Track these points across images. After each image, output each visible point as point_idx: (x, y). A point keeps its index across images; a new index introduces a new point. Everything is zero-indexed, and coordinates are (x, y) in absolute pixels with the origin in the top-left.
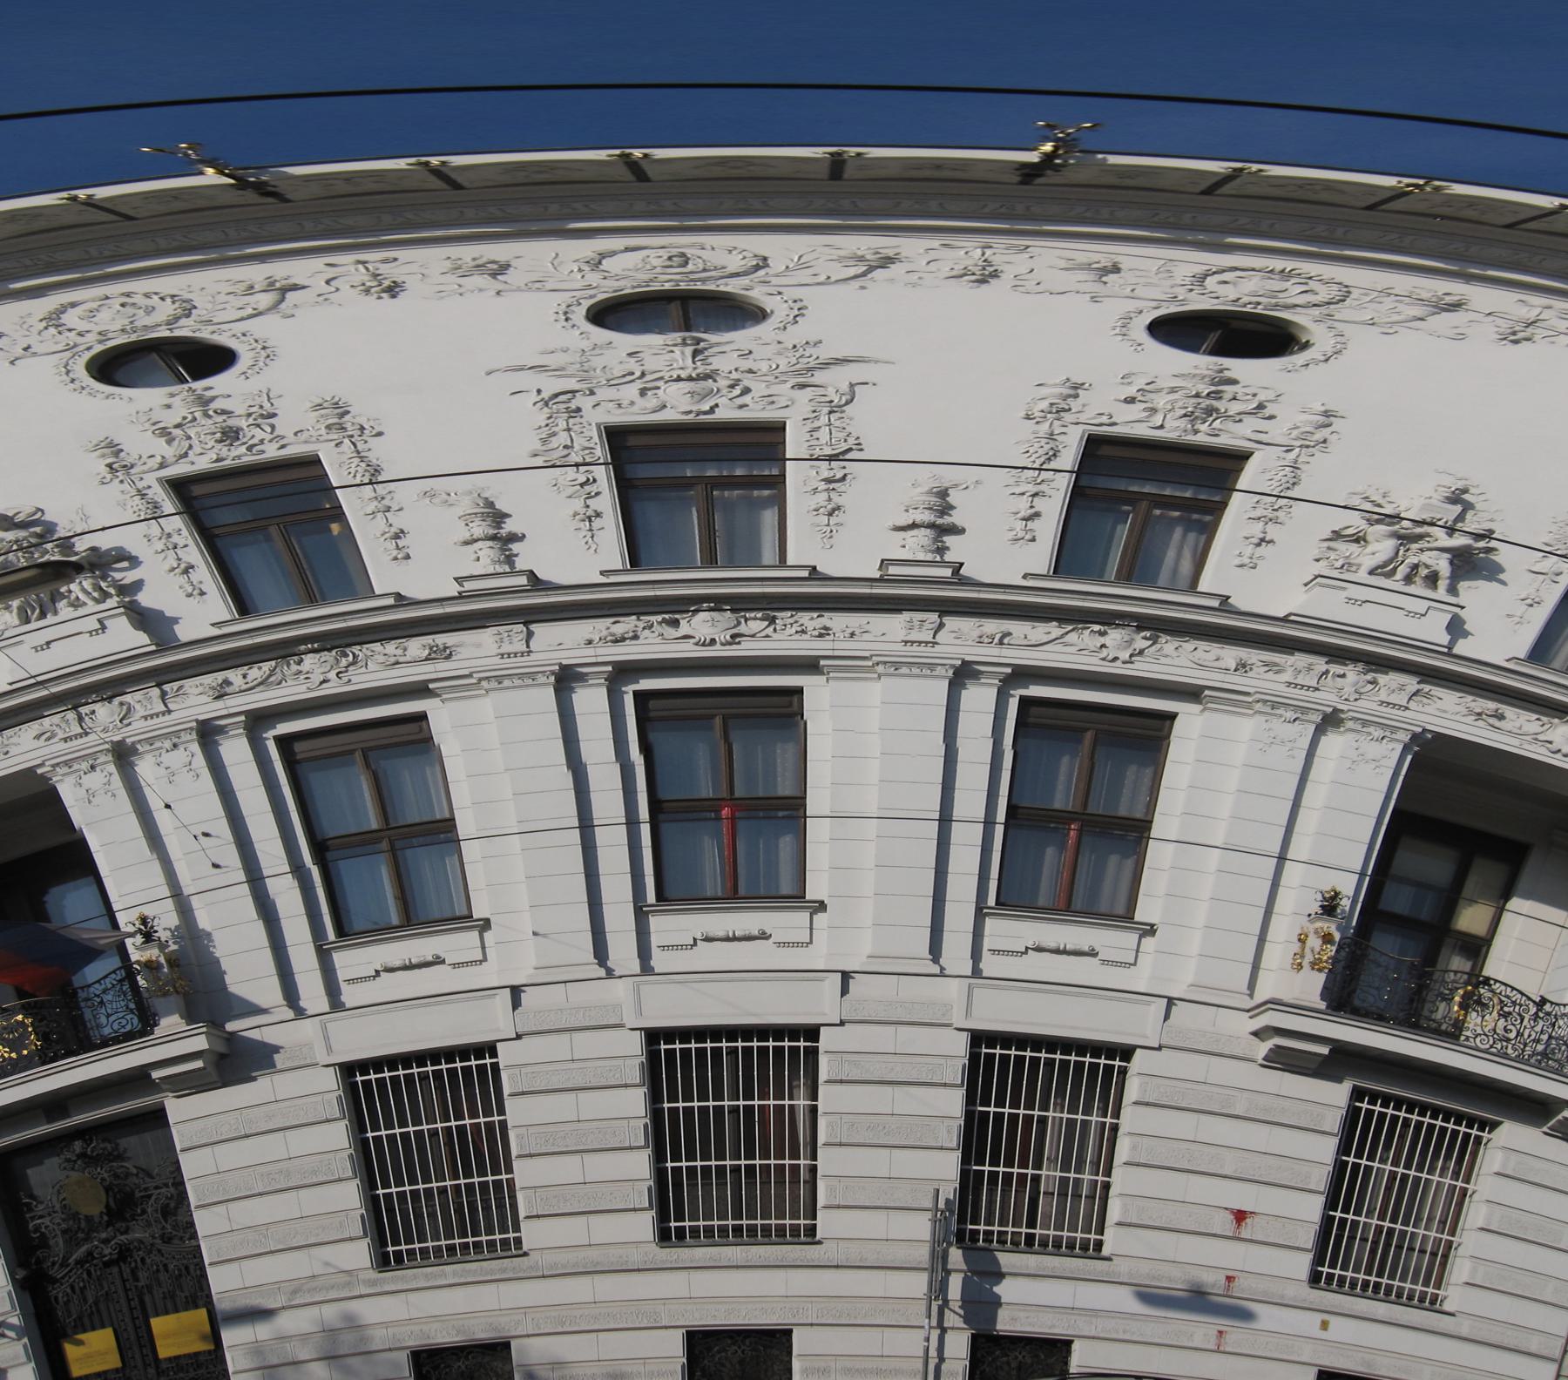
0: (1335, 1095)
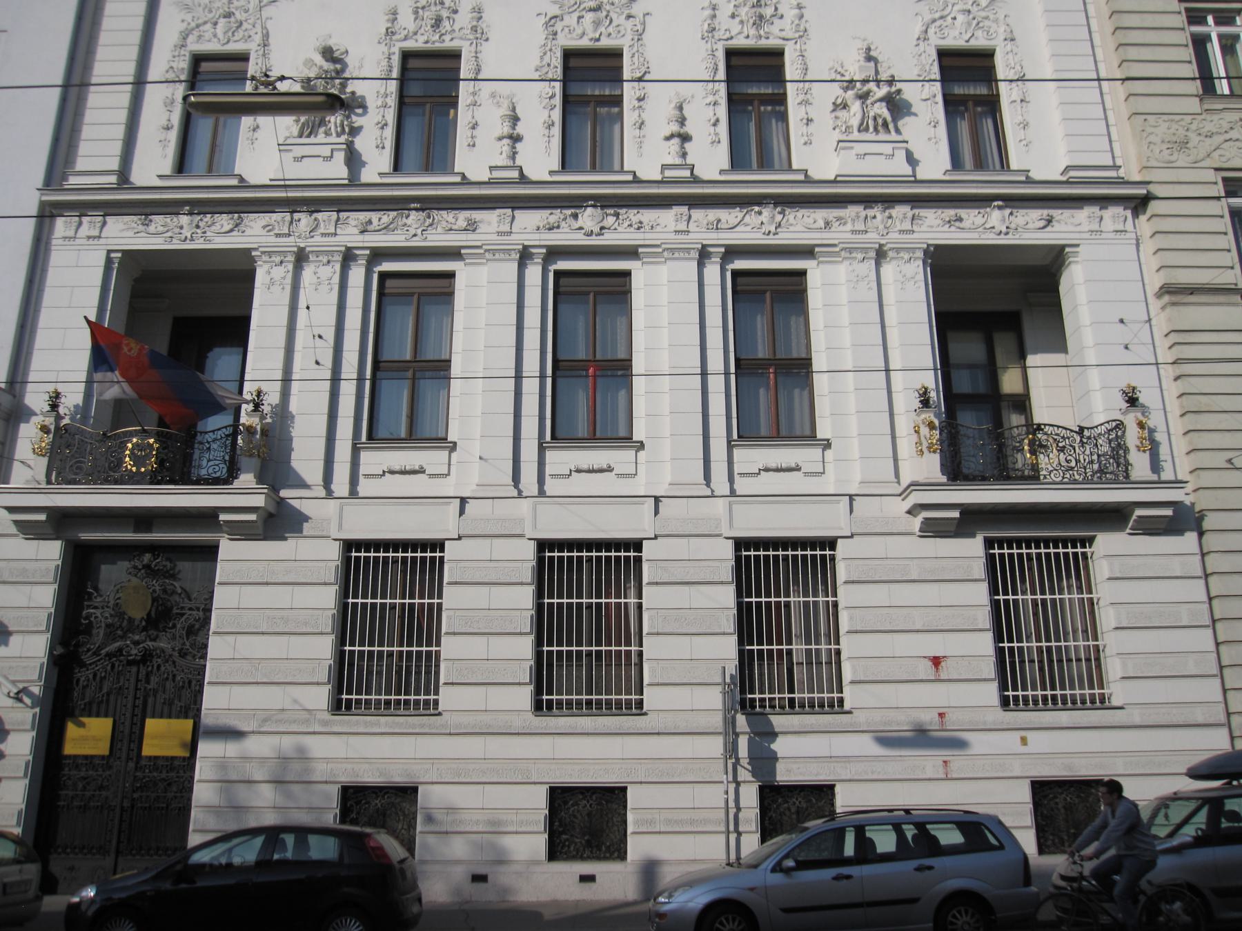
0: (974, 547)
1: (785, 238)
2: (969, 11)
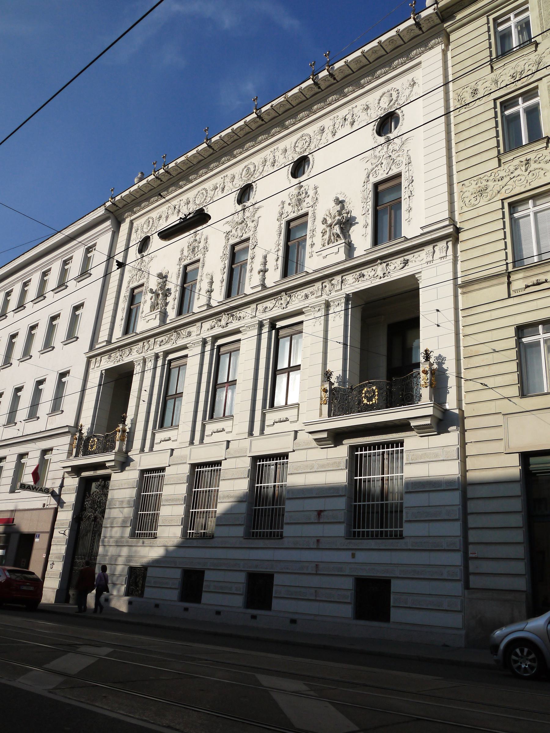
1: (291, 308)
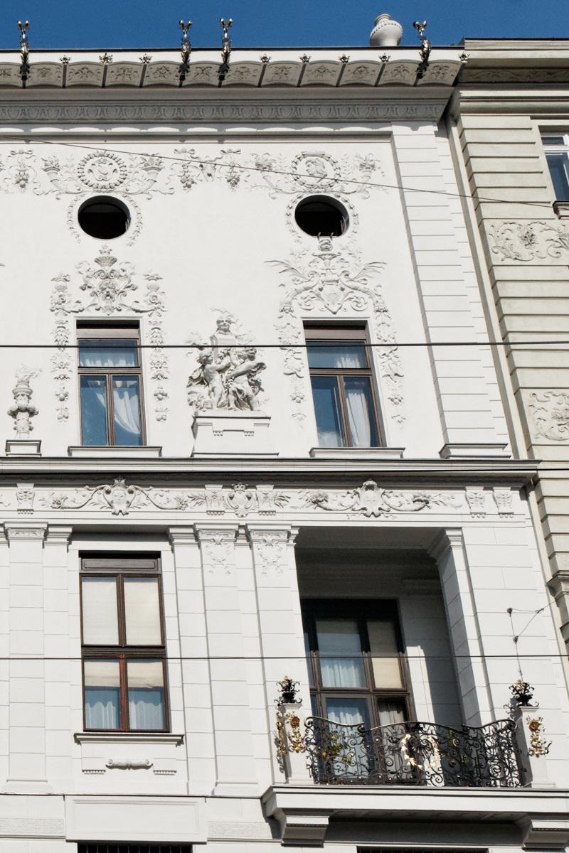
2: (337, 281)
